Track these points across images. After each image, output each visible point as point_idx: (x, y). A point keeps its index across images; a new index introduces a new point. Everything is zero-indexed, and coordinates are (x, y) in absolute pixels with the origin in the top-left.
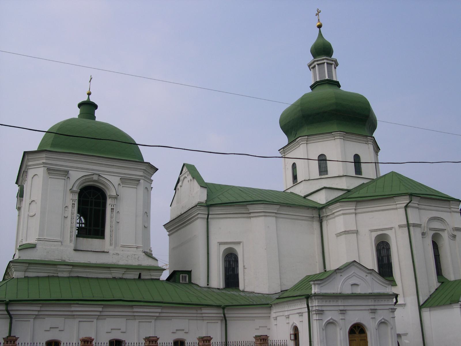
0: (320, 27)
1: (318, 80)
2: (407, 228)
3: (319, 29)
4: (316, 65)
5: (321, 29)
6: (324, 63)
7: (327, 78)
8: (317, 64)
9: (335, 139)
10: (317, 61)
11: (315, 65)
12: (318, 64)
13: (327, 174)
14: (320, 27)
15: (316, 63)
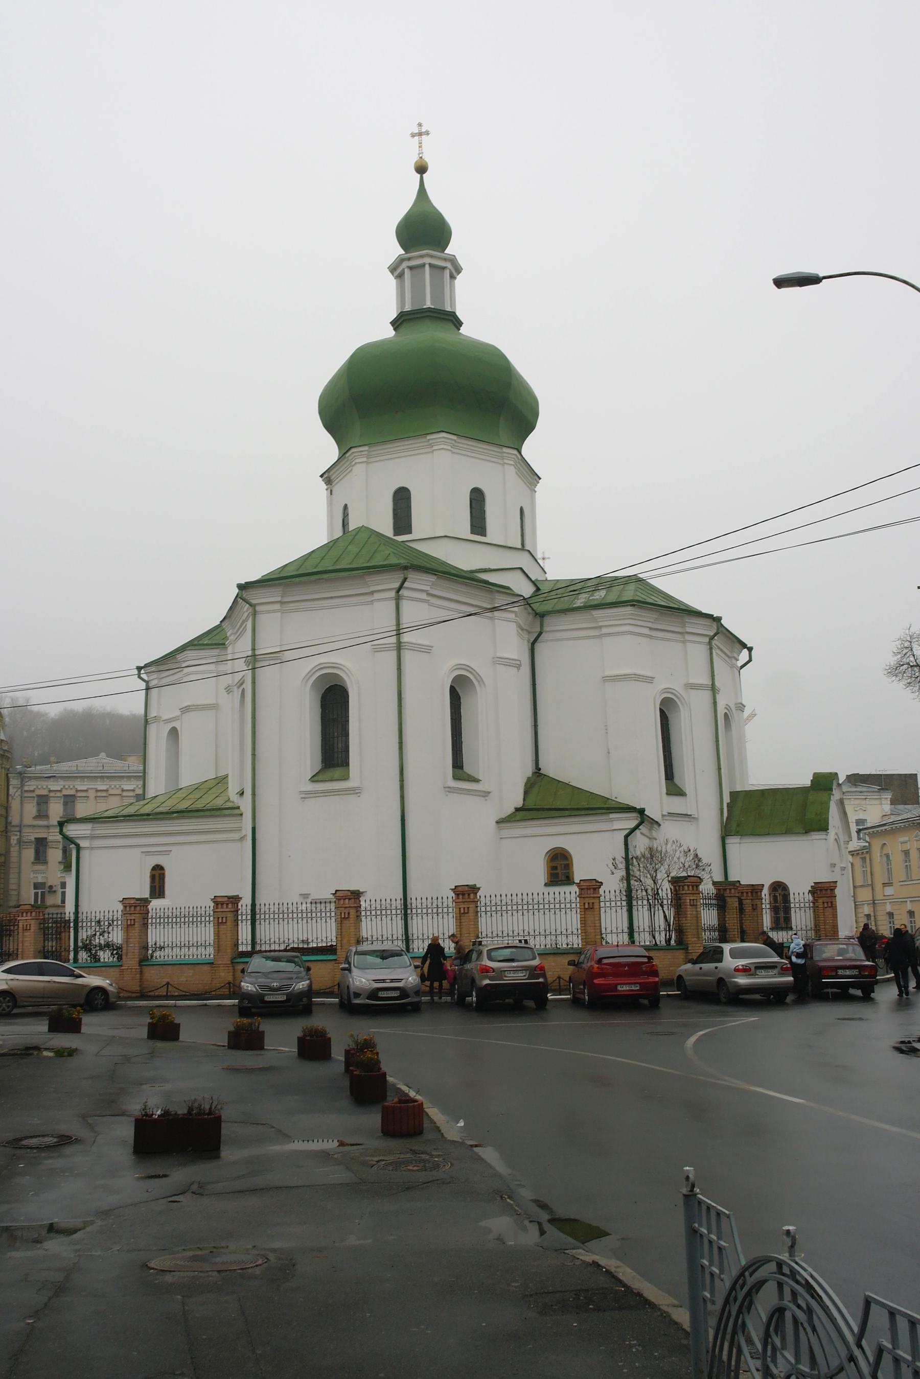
0: (421, 169)
1: (428, 304)
2: (707, 694)
3: (419, 175)
4: (427, 267)
5: (424, 175)
6: (444, 268)
7: (448, 309)
8: (430, 265)
9: (432, 452)
10: (432, 256)
11: (423, 266)
12: (430, 265)
13: (485, 536)
14: (421, 169)
15: (427, 260)
